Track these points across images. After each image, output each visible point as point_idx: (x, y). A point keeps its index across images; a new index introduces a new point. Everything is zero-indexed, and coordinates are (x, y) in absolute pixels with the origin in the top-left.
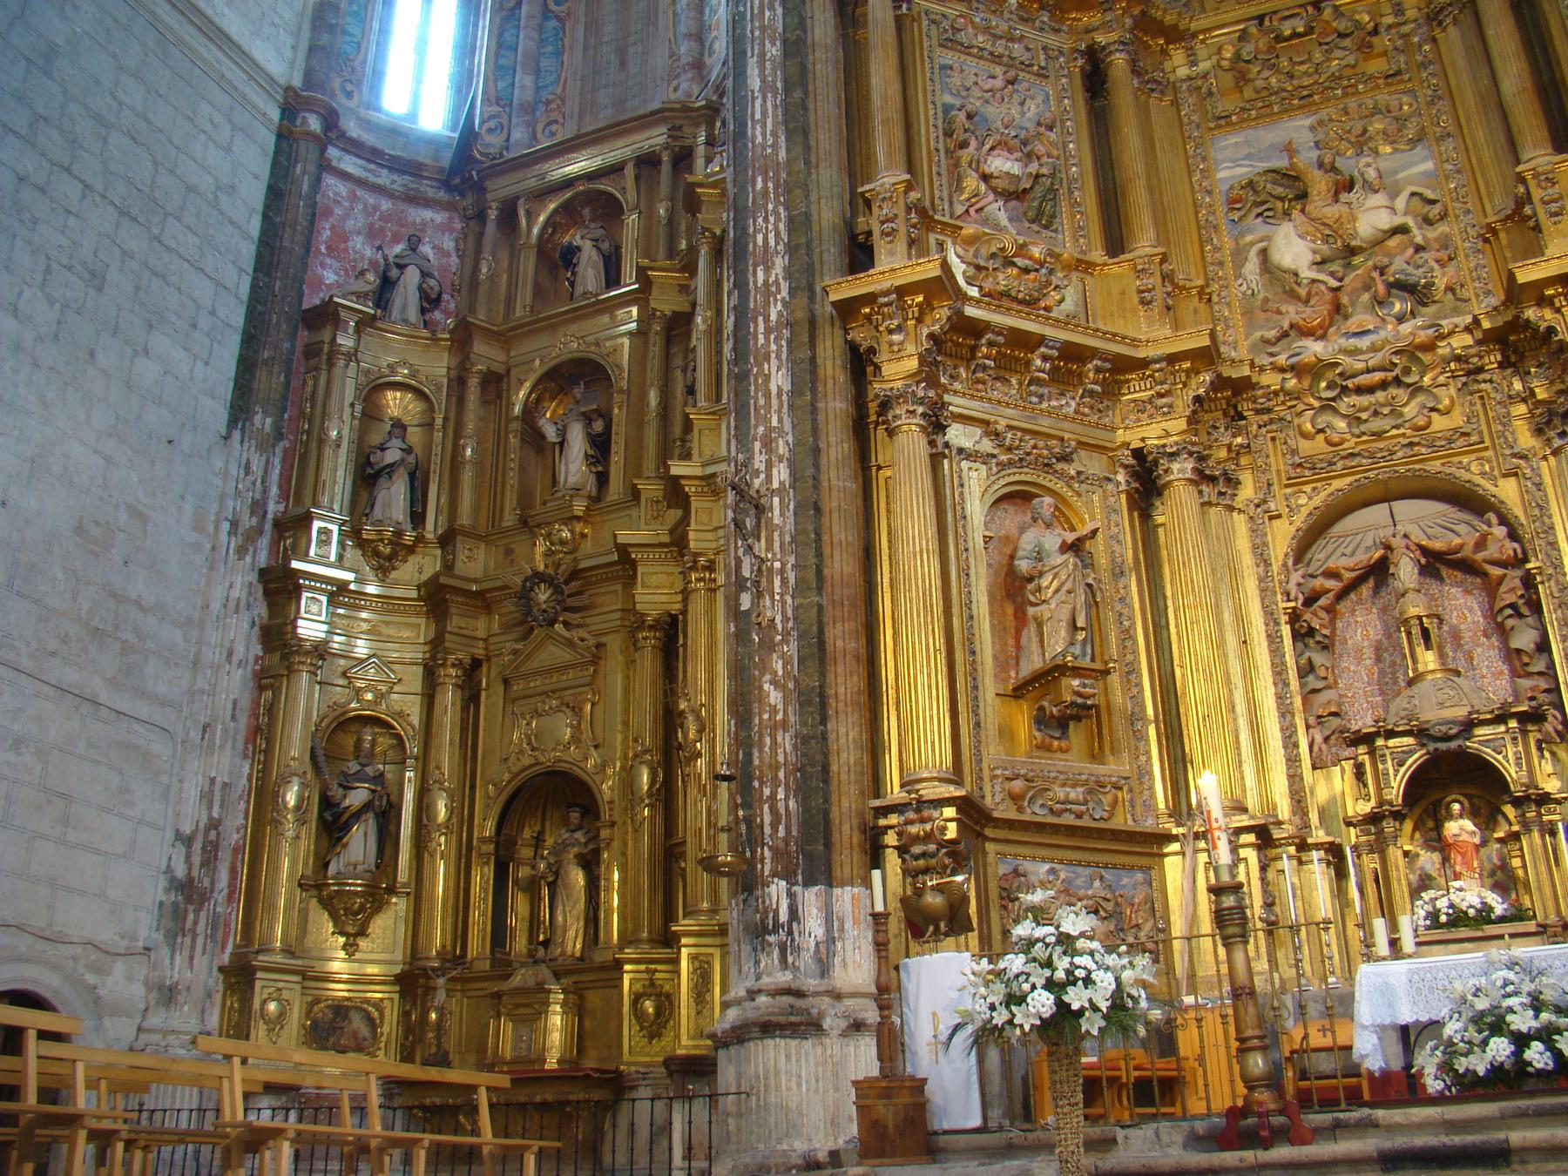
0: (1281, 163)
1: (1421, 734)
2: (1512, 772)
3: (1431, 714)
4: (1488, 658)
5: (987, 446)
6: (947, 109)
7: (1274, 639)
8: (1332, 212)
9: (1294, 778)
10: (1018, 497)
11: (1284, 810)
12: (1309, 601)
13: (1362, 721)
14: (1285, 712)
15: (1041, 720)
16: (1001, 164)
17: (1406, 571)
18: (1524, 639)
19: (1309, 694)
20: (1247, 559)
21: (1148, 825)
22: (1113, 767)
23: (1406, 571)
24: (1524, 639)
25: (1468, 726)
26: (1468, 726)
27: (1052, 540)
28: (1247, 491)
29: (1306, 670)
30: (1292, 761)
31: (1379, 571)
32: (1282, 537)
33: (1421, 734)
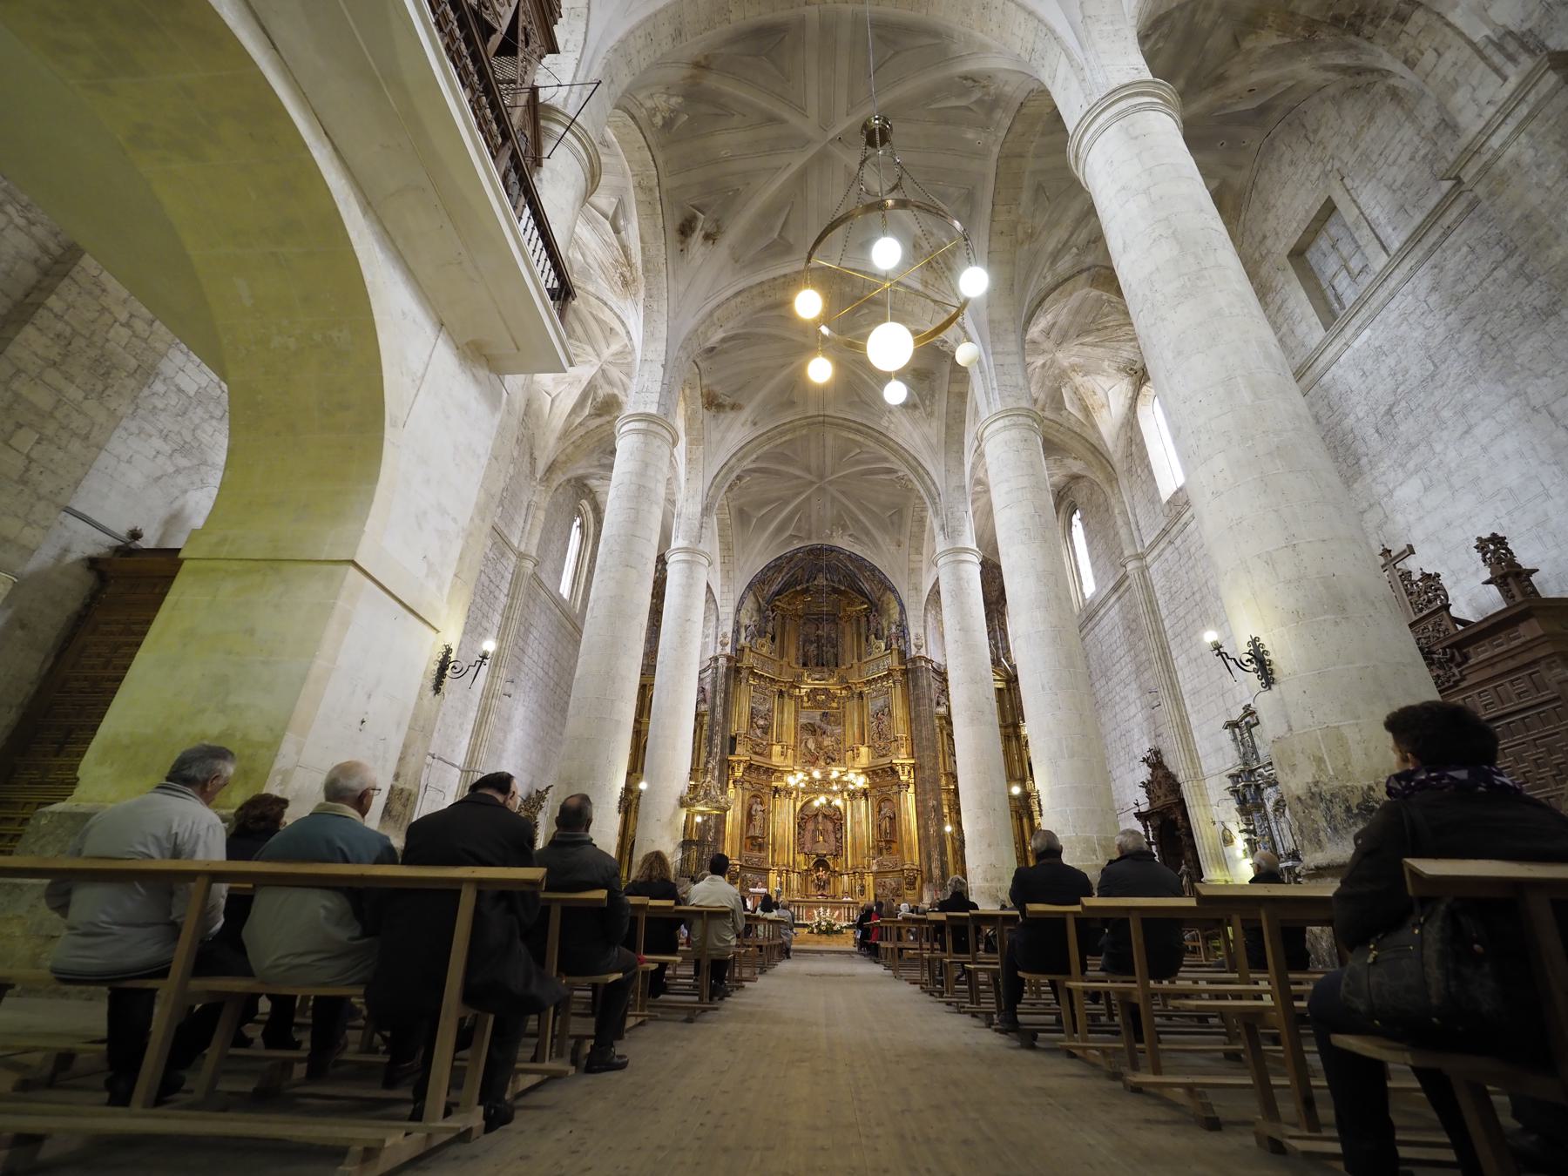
0: (812, 722)
1: (817, 855)
2: (831, 865)
3: (820, 852)
4: (832, 838)
5: (750, 787)
6: (753, 708)
7: (794, 827)
8: (820, 739)
9: (794, 857)
10: (754, 796)
11: (791, 863)
12: (802, 819)
13: (806, 850)
14: (794, 843)
15: (752, 844)
16: (761, 722)
17: (820, 818)
18: (839, 836)
19: (799, 839)
20: (792, 811)
21: (767, 867)
22: (763, 854)
23: (820, 818)
24: (839, 836)
25: (825, 855)
26: (825, 855)
27: (759, 808)
28: (794, 795)
29: (799, 833)
30: (794, 853)
31: (816, 815)
32: (799, 805)
33: (817, 855)
